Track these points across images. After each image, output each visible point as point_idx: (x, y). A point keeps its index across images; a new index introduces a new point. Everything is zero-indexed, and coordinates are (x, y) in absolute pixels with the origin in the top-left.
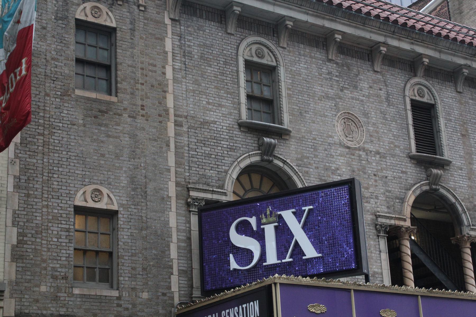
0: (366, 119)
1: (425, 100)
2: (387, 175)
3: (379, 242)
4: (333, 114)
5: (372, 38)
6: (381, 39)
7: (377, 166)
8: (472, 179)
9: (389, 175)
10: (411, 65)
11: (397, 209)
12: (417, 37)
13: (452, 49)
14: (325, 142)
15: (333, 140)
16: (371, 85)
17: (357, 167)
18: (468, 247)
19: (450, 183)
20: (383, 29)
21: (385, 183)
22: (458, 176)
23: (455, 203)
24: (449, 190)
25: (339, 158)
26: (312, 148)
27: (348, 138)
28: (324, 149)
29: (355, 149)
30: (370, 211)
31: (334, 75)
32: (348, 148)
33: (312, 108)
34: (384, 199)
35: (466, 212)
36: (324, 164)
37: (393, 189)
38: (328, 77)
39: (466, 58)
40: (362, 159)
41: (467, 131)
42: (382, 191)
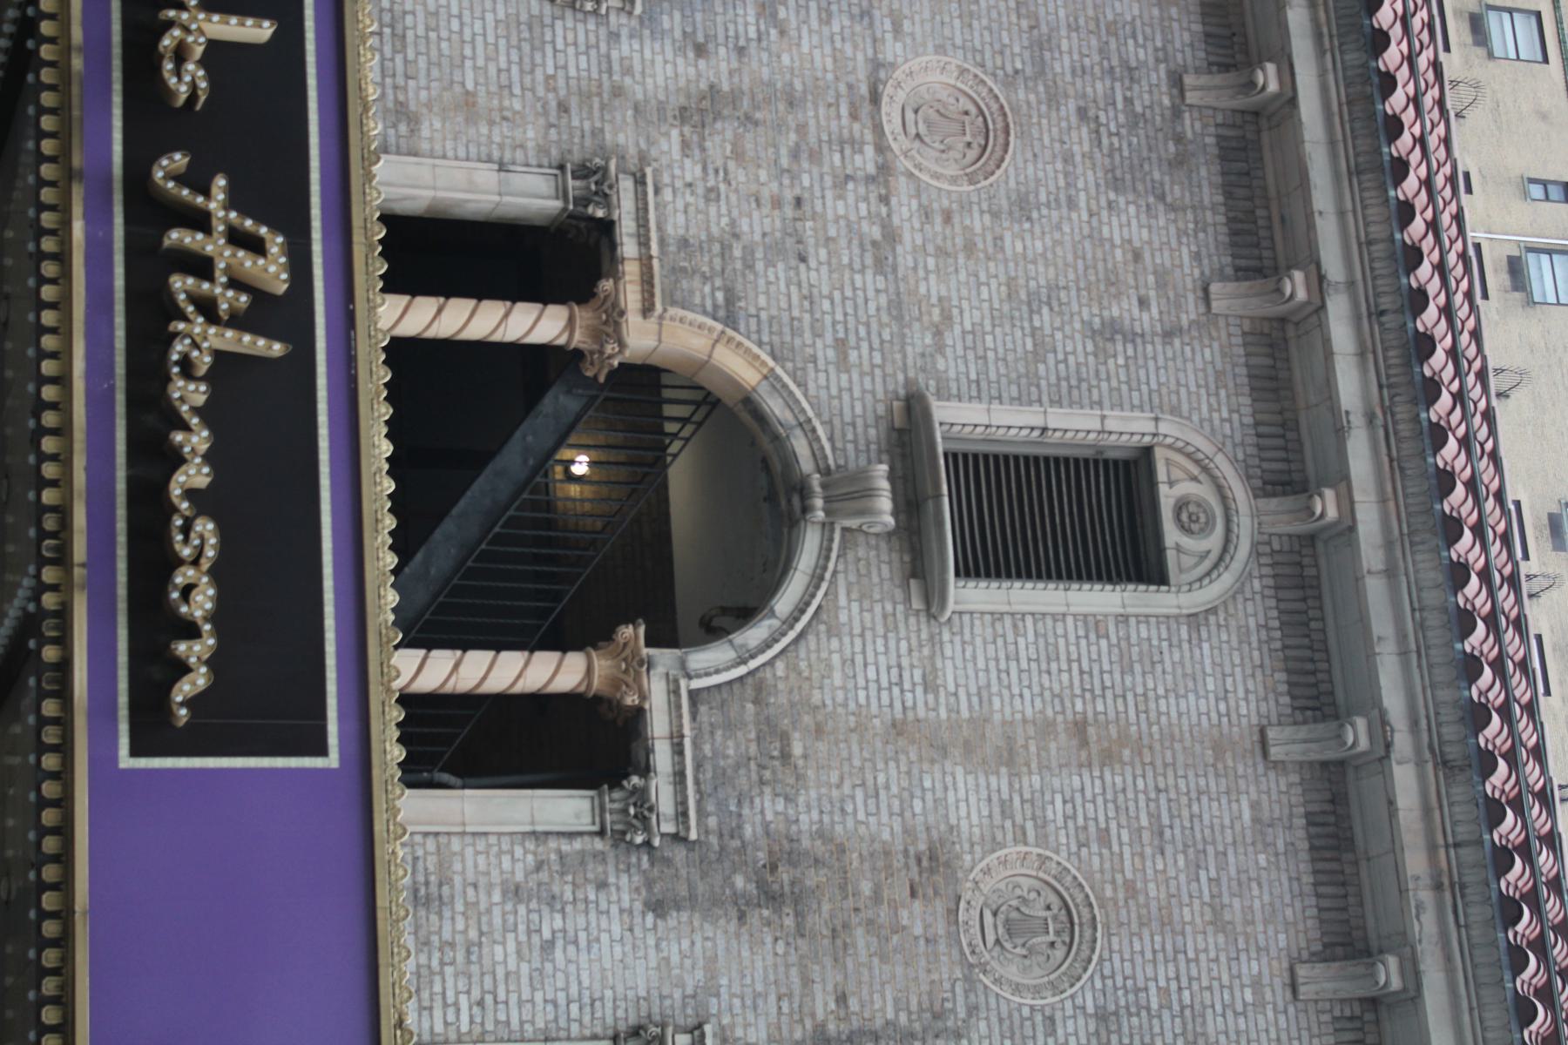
0: (1004, 203)
1: (1172, 535)
2: (813, 264)
3: (540, 166)
4: (982, 52)
5: (1318, 221)
6: (1333, 266)
7: (837, 221)
8: (901, 742)
9: (813, 274)
10: (1278, 365)
11: (685, 284)
12: (1405, 429)
13: (1421, 626)
15: (889, 36)
16: (1147, 255)
17: (812, 122)
18: (589, 671)
19: (855, 606)
20: (1372, 260)
21: (775, 251)
22: (893, 662)
23: (773, 614)
24: (822, 578)
25: (828, 49)
27: (910, 115)
29: (878, 129)
30: (654, 153)
31: (1130, 89)
32: (875, 98)
34: (715, 230)
35: (744, 662)
37: (761, 282)
38: (1115, 62)
39: (1414, 724)
40: (848, 152)
41: (1109, 758)
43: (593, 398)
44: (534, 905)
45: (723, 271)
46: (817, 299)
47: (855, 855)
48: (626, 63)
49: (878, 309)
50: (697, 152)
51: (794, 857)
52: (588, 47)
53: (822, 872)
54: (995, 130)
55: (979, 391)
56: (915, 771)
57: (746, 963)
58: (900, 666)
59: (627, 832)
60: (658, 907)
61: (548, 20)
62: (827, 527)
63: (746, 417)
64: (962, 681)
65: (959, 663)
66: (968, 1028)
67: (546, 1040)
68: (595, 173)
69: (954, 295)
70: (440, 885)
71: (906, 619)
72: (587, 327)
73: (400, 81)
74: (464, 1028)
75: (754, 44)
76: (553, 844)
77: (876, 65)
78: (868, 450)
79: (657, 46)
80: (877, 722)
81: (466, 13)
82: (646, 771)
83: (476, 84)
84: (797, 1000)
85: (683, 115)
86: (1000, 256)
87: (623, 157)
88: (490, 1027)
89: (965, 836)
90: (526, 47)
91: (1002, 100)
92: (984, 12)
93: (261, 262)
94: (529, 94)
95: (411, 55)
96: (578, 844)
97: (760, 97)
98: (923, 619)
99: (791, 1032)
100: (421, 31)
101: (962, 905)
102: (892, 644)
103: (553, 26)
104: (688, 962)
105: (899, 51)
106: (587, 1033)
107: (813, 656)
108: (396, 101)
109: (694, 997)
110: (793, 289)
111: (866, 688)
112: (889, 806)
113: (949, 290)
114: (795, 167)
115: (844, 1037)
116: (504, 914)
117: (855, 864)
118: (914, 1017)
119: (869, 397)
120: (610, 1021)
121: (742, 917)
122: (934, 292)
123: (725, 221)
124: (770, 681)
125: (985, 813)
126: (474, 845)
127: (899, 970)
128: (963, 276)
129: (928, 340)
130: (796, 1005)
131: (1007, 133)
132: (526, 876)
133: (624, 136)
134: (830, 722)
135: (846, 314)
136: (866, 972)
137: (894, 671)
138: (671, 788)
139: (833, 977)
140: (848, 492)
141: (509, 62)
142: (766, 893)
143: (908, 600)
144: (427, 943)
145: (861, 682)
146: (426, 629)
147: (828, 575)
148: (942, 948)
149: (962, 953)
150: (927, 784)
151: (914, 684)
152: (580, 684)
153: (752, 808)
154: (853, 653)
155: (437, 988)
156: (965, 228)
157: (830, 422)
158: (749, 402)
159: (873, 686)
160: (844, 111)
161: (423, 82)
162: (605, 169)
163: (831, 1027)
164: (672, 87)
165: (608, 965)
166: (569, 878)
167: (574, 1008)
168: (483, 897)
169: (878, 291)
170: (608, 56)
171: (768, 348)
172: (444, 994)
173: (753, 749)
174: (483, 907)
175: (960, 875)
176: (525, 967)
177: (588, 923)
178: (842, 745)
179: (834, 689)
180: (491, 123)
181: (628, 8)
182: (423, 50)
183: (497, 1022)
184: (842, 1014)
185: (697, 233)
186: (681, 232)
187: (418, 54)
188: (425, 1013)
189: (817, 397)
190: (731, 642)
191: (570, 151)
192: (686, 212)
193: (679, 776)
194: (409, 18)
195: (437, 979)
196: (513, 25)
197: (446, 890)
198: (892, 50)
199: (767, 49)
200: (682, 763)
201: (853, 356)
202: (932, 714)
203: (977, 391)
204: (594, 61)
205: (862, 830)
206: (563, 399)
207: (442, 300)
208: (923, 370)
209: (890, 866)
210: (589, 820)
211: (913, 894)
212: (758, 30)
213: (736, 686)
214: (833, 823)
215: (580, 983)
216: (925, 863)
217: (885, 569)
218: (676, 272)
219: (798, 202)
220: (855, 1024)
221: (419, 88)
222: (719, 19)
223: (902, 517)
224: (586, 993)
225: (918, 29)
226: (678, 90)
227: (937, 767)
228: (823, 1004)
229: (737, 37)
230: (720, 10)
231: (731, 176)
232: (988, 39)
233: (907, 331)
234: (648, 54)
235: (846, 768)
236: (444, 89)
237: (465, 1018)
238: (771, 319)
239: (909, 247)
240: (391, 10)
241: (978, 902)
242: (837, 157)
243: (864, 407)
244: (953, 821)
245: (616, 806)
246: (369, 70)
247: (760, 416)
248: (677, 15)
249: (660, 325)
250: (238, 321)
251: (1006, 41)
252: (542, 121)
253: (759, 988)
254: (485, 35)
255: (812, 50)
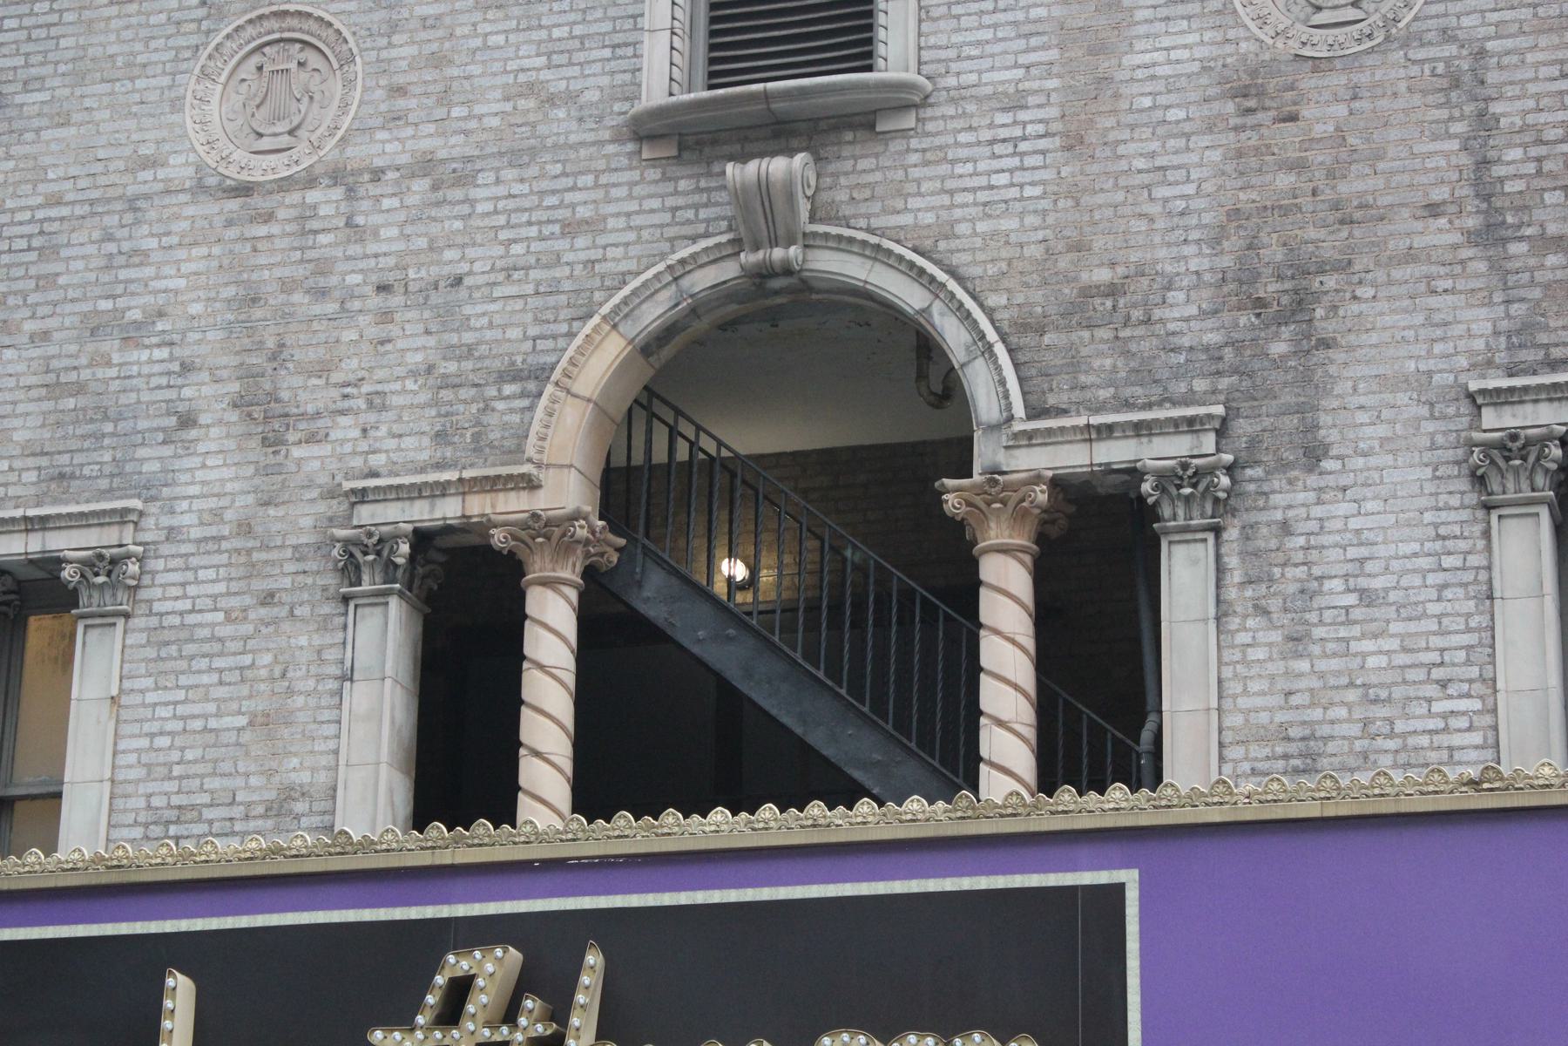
2: (465, 267)
3: (345, 627)
4: (178, 49)
8: (1092, 137)
9: (477, 267)
11: (494, 435)
14: (109, 201)
15: (161, 174)
17: (278, 273)
18: (1004, 550)
19: (914, 203)
22: (986, 151)
23: (925, 311)
24: (878, 247)
25: (181, 254)
26: (29, 249)
28: (96, 235)
29: (285, 184)
30: (323, 479)
32: (244, 190)
33: (70, 54)
34: (423, 397)
35: (990, 347)
36: (85, 307)
37: (489, 335)
42: (419, 357)
43: (647, 552)
44: (1313, 617)
45: (476, 385)
46: (510, 262)
47: (1242, 196)
48: (207, 517)
49: (522, 180)
50: (320, 423)
51: (1246, 276)
52: (187, 569)
53: (1266, 240)
54: (282, 30)
55: (626, 45)
56: (1130, 119)
57: (1386, 336)
58: (992, 142)
59: (1214, 496)
60: (1314, 455)
61: (154, 621)
62: (810, 242)
63: (668, 352)
64: (1010, 59)
65: (987, 63)
66: (1470, 41)
67: (1491, 597)
68: (352, 555)
69: (499, 80)
70: (1288, 739)
71: (928, 134)
72: (554, 561)
73: (237, 811)
74: (1476, 705)
75: (177, 351)
76: (1231, 593)
77: (200, 189)
78: (708, 190)
79: (184, 478)
80: (1065, 172)
81: (147, 727)
82: (1134, 473)
83: (240, 713)
84: (1434, 269)
85: (272, 442)
86: (447, 20)
87: (331, 519)
88: (1474, 672)
89: (1216, 51)
90: (190, 649)
91: (240, 22)
92: (126, 48)
93: (480, 982)
94: (251, 644)
95: (206, 798)
96: (1232, 561)
97: (246, 341)
98: (929, 112)
99: (1477, 276)
100: (171, 786)
101: (1307, 52)
102: (963, 153)
103: (161, 615)
104: (1386, 414)
105: (181, 159)
106: (1481, 544)
107: (980, 256)
108: (265, 816)
109: (1432, 405)
110: (498, 292)
111: (1021, 186)
112: (1176, 153)
113: (493, 87)
114: (337, 294)
115: (1485, 206)
116: (1325, 655)
117: (1254, 195)
118: (1457, 113)
119: (637, 190)
120: (1465, 515)
121: (1326, 344)
122: (496, 107)
123: (410, 385)
124: (1015, 312)
125: (1185, 23)
126: (1235, 697)
127: (1394, 134)
128: (476, 70)
129: (561, 114)
130: (1442, 270)
131: (286, 13)
132: (1276, 628)
133: (304, 518)
134: (1067, 233)
135: (530, 223)
136: (1397, 178)
137: (999, 149)
138: (1156, 440)
139: (1404, 221)
140: (762, 215)
141: (210, 670)
142: (1293, 313)
143: (904, 133)
144: (1365, 755)
145: (1014, 192)
146: (957, 765)
147: (874, 240)
148: (1363, 78)
149: (1371, 51)
150: (1147, 102)
151: (1015, 123)
152: (1021, 562)
153: (1181, 333)
154: (975, 204)
155: (1424, 741)
156: (411, 67)
157: (671, 240)
158: (647, 348)
159: (1019, 177)
160: (262, 230)
161: (239, 782)
162: (347, 542)
163: (1471, 222)
164: (237, 458)
165: (1392, 518)
166: (1277, 571)
167: (1447, 562)
168: (1303, 684)
169: (498, 181)
170: (199, 541)
171: (576, 324)
172: (1430, 732)
173: (1104, 333)
174: (1316, 683)
175: (1267, 57)
176: (1395, 628)
177: (1336, 545)
178: (1097, 217)
179: (1023, 228)
180: (290, 692)
181: (134, 517)
182: (197, 782)
183: (1468, 662)
184: (1453, 209)
185: (428, 421)
186: (426, 441)
187: (202, 789)
188: (1457, 756)
189: (639, 259)
190: (962, 366)
191: (325, 589)
192: (400, 436)
193: (1140, 430)
194: (157, 802)
195: (1411, 741)
196: (162, 666)
197: (1294, 732)
198: (179, 169)
199: (184, 333)
200: (1123, 426)
201: (583, 212)
202: (1054, 96)
203: (626, 47)
204: (205, 560)
205: (1208, 187)
206: (646, 593)
207: (522, 751)
208: (600, 119)
209: (1257, 149)
210: (1200, 546)
211: (1293, 118)
212: (159, 346)
213: (1021, 358)
214: (1199, 226)
215: (1415, 555)
216: (1252, 103)
217: (863, 164)
218: (478, 446)
219: (383, 288)
220: (1466, 191)
221: (247, 787)
222: (146, 397)
223: (795, 143)
224: (1428, 545)
225: (149, 136)
226: (240, 448)
227: (1124, 90)
228: (1440, 235)
229: (169, 373)
230: (134, 395)
231: (352, 377)
232: (162, 41)
233: (549, 142)
234: (194, 490)
235: (1127, 210)
236: (247, 754)
237: (1463, 705)
238: (537, 321)
239: (439, 142)
240: (146, 825)
241: (1303, 32)
242: (323, 239)
243: (650, 196)
244: (1196, 67)
245: (1181, 512)
246: (226, 851)
247: (666, 334)
248: (142, 452)
249: (548, 466)
250: (559, 1011)
251: (163, 17)
252: (286, 626)
253: (1419, 319)
254: (176, 703)
255: (182, 275)
